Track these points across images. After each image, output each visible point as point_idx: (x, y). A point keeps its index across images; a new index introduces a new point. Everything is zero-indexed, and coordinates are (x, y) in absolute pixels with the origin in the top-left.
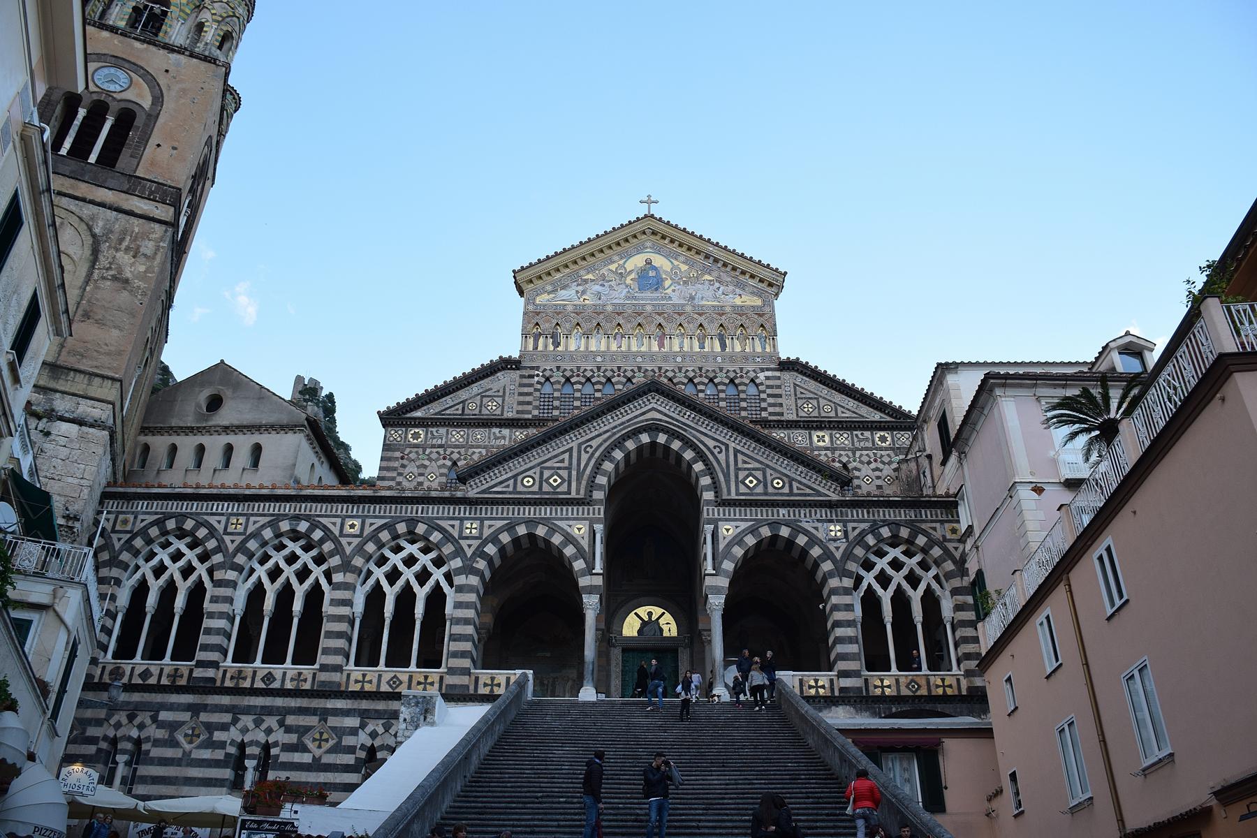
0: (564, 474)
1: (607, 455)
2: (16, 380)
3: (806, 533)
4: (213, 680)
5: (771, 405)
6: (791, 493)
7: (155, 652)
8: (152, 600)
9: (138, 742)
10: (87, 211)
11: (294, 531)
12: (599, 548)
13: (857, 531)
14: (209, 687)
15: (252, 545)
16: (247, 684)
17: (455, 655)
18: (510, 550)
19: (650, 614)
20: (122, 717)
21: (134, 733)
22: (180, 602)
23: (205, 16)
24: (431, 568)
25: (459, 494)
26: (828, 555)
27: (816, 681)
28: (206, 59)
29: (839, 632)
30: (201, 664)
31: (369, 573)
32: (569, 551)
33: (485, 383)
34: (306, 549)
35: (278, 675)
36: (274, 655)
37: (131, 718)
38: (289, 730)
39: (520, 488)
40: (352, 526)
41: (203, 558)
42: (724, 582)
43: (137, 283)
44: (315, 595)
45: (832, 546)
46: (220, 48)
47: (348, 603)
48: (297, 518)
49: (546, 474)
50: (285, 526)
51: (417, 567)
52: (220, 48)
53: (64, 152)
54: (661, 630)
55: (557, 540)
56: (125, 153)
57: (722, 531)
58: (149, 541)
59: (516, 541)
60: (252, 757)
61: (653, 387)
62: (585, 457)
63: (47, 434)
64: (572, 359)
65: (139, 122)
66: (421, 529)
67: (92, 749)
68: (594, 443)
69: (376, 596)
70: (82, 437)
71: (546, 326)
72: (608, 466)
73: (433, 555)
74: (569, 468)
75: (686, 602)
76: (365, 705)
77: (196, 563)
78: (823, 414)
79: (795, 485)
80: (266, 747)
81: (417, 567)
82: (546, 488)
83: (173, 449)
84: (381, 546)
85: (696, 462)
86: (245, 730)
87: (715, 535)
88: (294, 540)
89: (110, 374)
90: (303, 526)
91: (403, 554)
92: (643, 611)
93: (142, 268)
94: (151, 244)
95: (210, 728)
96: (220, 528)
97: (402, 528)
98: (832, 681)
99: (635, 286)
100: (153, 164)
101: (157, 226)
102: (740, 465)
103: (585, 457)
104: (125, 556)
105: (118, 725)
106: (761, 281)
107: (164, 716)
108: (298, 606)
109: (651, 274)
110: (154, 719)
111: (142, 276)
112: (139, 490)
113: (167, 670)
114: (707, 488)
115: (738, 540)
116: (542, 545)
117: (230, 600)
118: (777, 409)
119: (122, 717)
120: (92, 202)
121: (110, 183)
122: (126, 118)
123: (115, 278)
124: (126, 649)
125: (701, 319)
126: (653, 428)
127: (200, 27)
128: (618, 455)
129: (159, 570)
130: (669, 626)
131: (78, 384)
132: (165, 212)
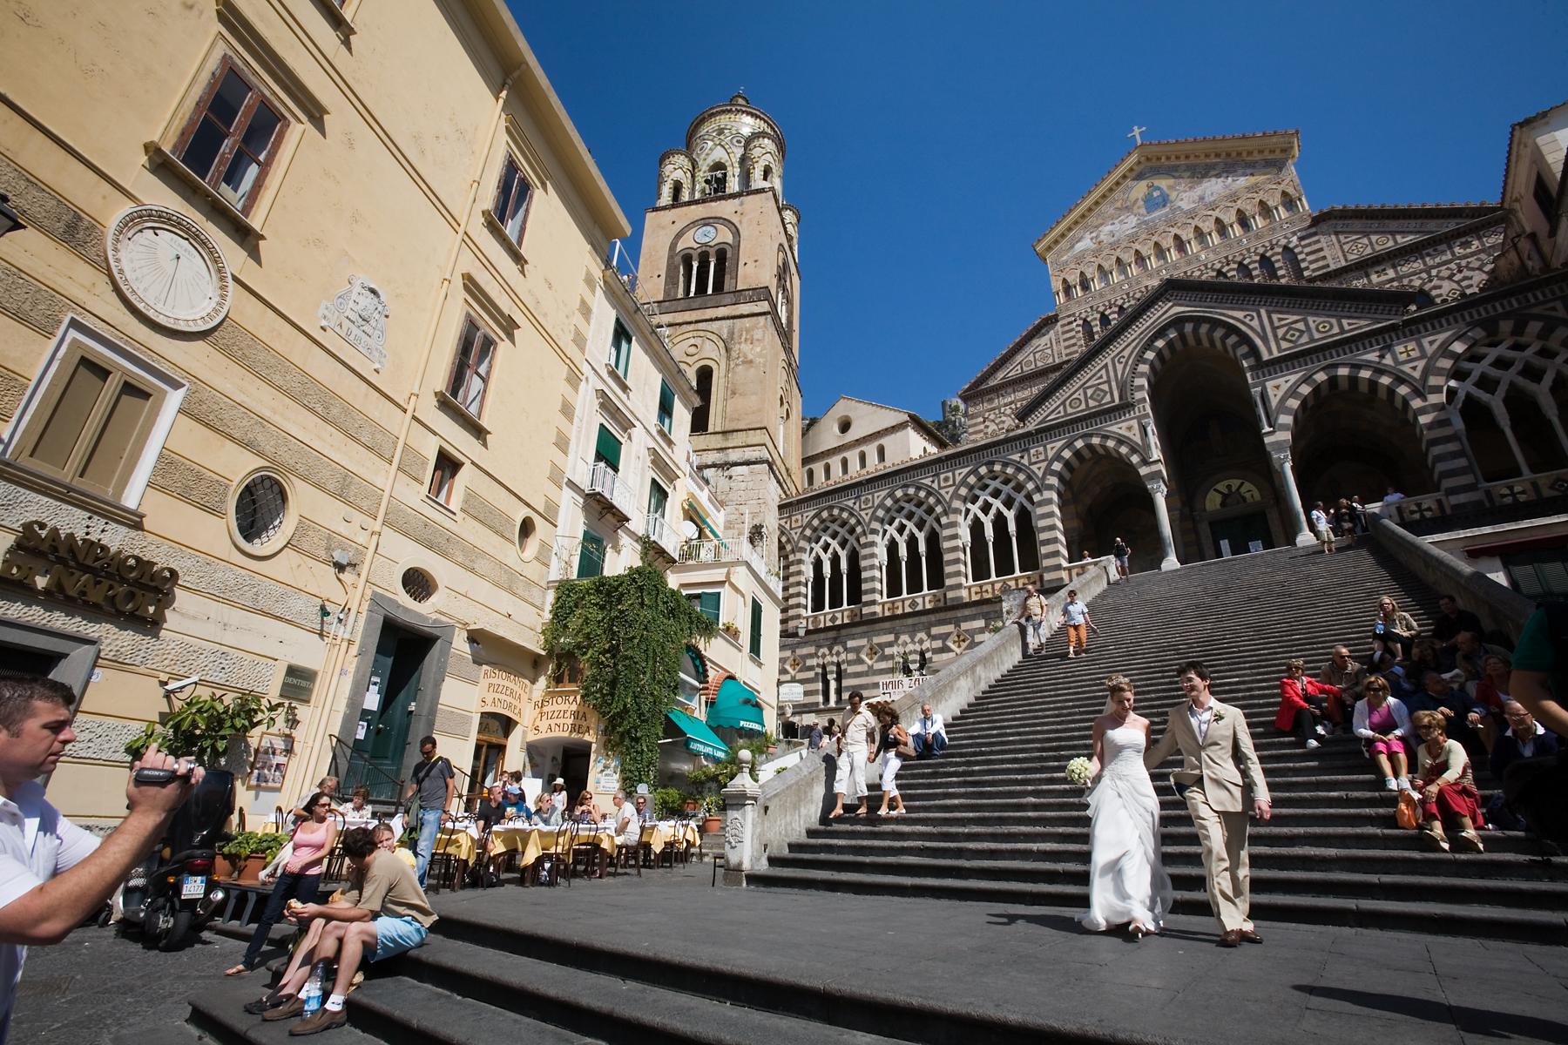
0: (1105, 387)
1: (1140, 359)
2: (670, 443)
3: (1367, 365)
5: (1311, 262)
6: (1343, 331)
7: (836, 602)
8: (827, 570)
9: (838, 665)
10: (715, 326)
12: (1154, 440)
13: (1435, 346)
14: (873, 621)
15: (881, 513)
16: (900, 612)
17: (1048, 556)
18: (1075, 463)
19: (1229, 487)
21: (835, 659)
22: (844, 566)
24: (1014, 494)
25: (1020, 431)
26: (1400, 379)
27: (1419, 505)
29: (1437, 450)
31: (968, 511)
32: (1124, 450)
33: (1035, 342)
34: (919, 504)
35: (920, 601)
36: (915, 587)
37: (830, 650)
38: (934, 638)
39: (1070, 410)
40: (946, 479)
42: (1286, 436)
44: (933, 540)
45: (1406, 368)
46: (765, 179)
47: (955, 537)
48: (906, 486)
49: (1089, 392)
50: (899, 493)
51: (1003, 496)
52: (765, 179)
54: (1244, 499)
55: (1111, 444)
56: (727, 277)
57: (1271, 392)
58: (815, 530)
59: (1077, 454)
60: (914, 662)
61: (1173, 288)
62: (1120, 367)
64: (1101, 295)
65: (729, 255)
66: (997, 468)
67: (811, 674)
68: (1126, 353)
69: (977, 527)
71: (1073, 278)
72: (1144, 368)
73: (1012, 484)
74: (1108, 382)
75: (1260, 464)
76: (986, 608)
77: (847, 536)
78: (1378, 248)
79: (1345, 322)
80: (922, 654)
81: (1003, 496)
82: (1092, 403)
84: (971, 488)
85: (1226, 336)
86: (905, 644)
87: (1264, 396)
88: (909, 501)
90: (911, 491)
91: (990, 490)
92: (1221, 486)
95: (882, 646)
97: (983, 470)
98: (1439, 502)
99: (1143, 211)
100: (745, 277)
102: (1277, 324)
103: (1120, 367)
105: (824, 656)
106: (1272, 151)
107: (850, 644)
108: (922, 548)
109: (1155, 194)
111: (760, 355)
114: (1245, 357)
115: (1292, 392)
116: (1101, 451)
117: (873, 555)
118: (1321, 263)
120: (717, 319)
122: (722, 256)
124: (818, 605)
125: (1216, 214)
126: (1178, 322)
128: (1150, 355)
130: (1250, 492)
132: (764, 306)
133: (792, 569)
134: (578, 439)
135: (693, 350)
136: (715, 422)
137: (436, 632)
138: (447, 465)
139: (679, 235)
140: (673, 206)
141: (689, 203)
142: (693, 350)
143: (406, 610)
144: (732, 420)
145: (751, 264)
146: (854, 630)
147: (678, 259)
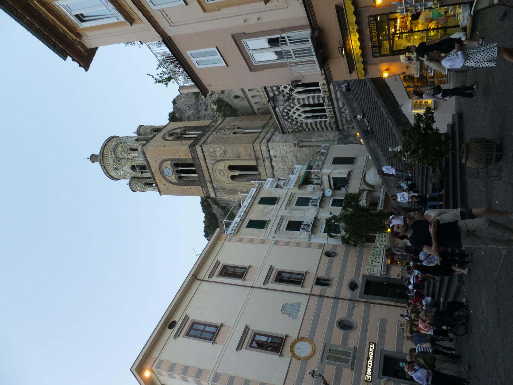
4: (328, 98)
7: (324, 111)
11: (277, 90)
14: (330, 98)
20: (344, 115)
22: (307, 109)
23: (129, 157)
28: (144, 153)
30: (324, 101)
37: (343, 112)
41: (293, 108)
43: (223, 148)
46: (136, 150)
48: (273, 91)
53: (197, 175)
56: (186, 162)
58: (293, 120)
63: (275, 156)
65: (176, 162)
70: (272, 149)
83: (256, 103)
88: (279, 88)
89: (252, 147)
93: (218, 149)
94: (210, 149)
96: (283, 107)
101: (204, 150)
104: (299, 124)
105: (346, 115)
107: (341, 106)
110: (343, 108)
111: (221, 148)
112: (279, 126)
113: (328, 107)
119: (344, 115)
121: (198, 162)
122: (176, 165)
123: (225, 154)
127: (133, 157)
129: (300, 115)
131: (258, 154)
132: (198, 148)
133: (309, 127)
134: (294, 238)
135: (222, 173)
136: (253, 163)
137: (365, 280)
138: (319, 282)
139: (171, 182)
140: (157, 185)
141: (155, 179)
142: (222, 173)
143: (361, 289)
144: (251, 157)
145: (179, 154)
146: (336, 105)
147: (181, 181)
